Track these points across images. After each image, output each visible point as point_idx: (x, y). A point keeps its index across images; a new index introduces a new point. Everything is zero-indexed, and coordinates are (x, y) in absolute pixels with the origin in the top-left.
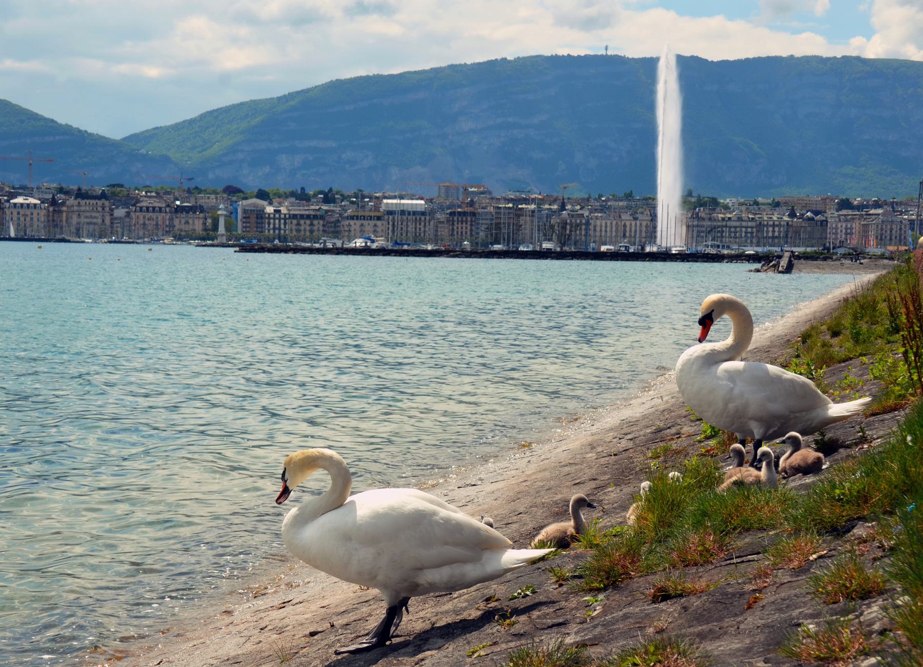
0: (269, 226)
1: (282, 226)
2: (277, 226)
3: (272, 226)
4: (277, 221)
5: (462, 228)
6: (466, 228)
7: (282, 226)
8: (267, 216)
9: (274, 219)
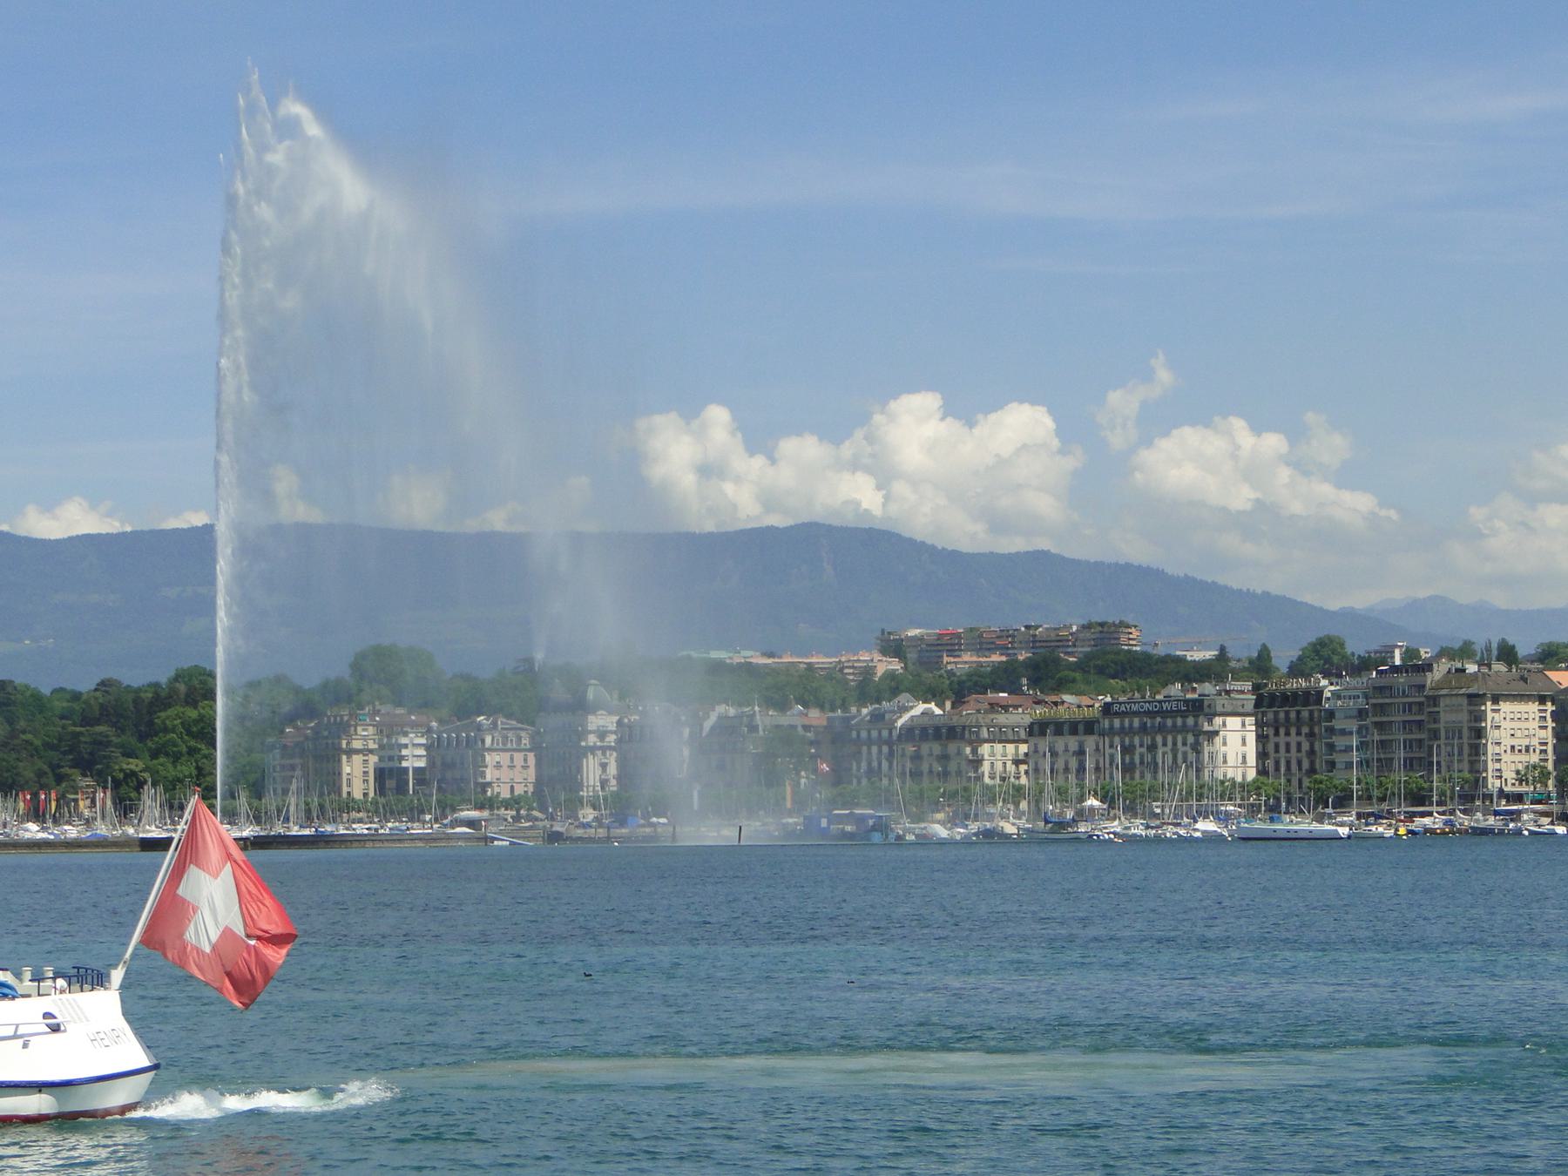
0: (859, 769)
1: (885, 765)
2: (875, 764)
3: (864, 765)
4: (875, 749)
5: (1288, 745)
6: (1299, 745)
7: (885, 765)
8: (854, 734)
9: (870, 742)
